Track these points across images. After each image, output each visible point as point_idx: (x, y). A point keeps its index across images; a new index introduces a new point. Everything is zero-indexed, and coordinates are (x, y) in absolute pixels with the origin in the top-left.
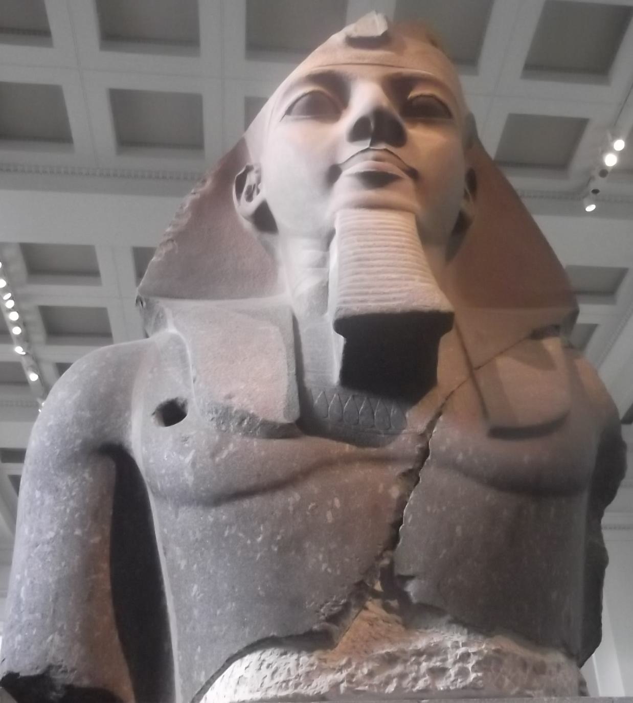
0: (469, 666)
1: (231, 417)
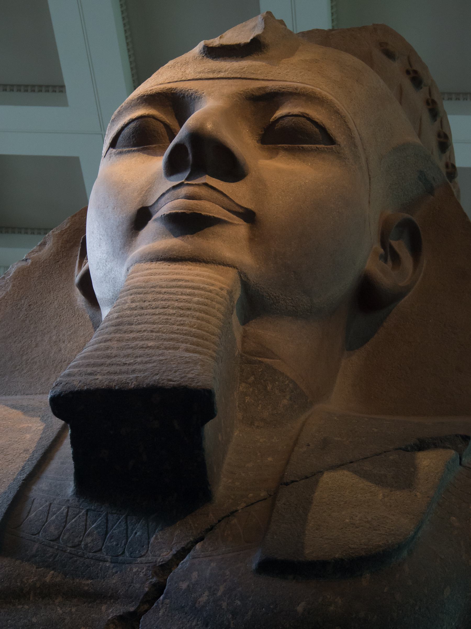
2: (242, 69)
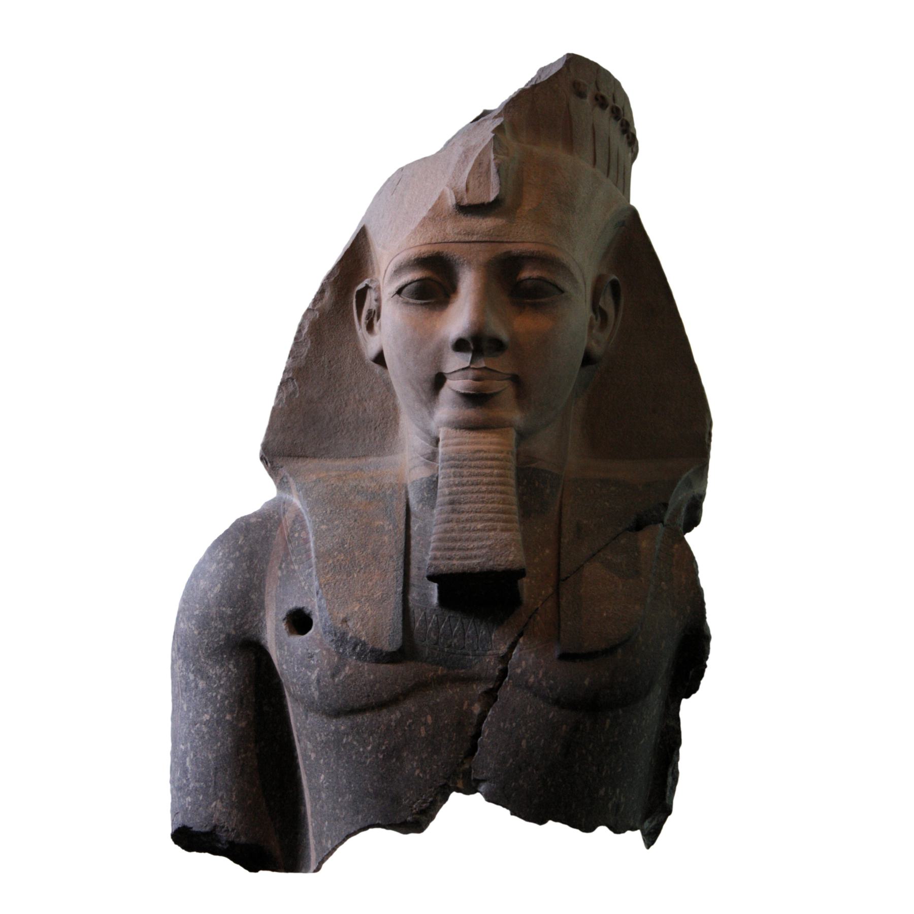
1: (347, 642)
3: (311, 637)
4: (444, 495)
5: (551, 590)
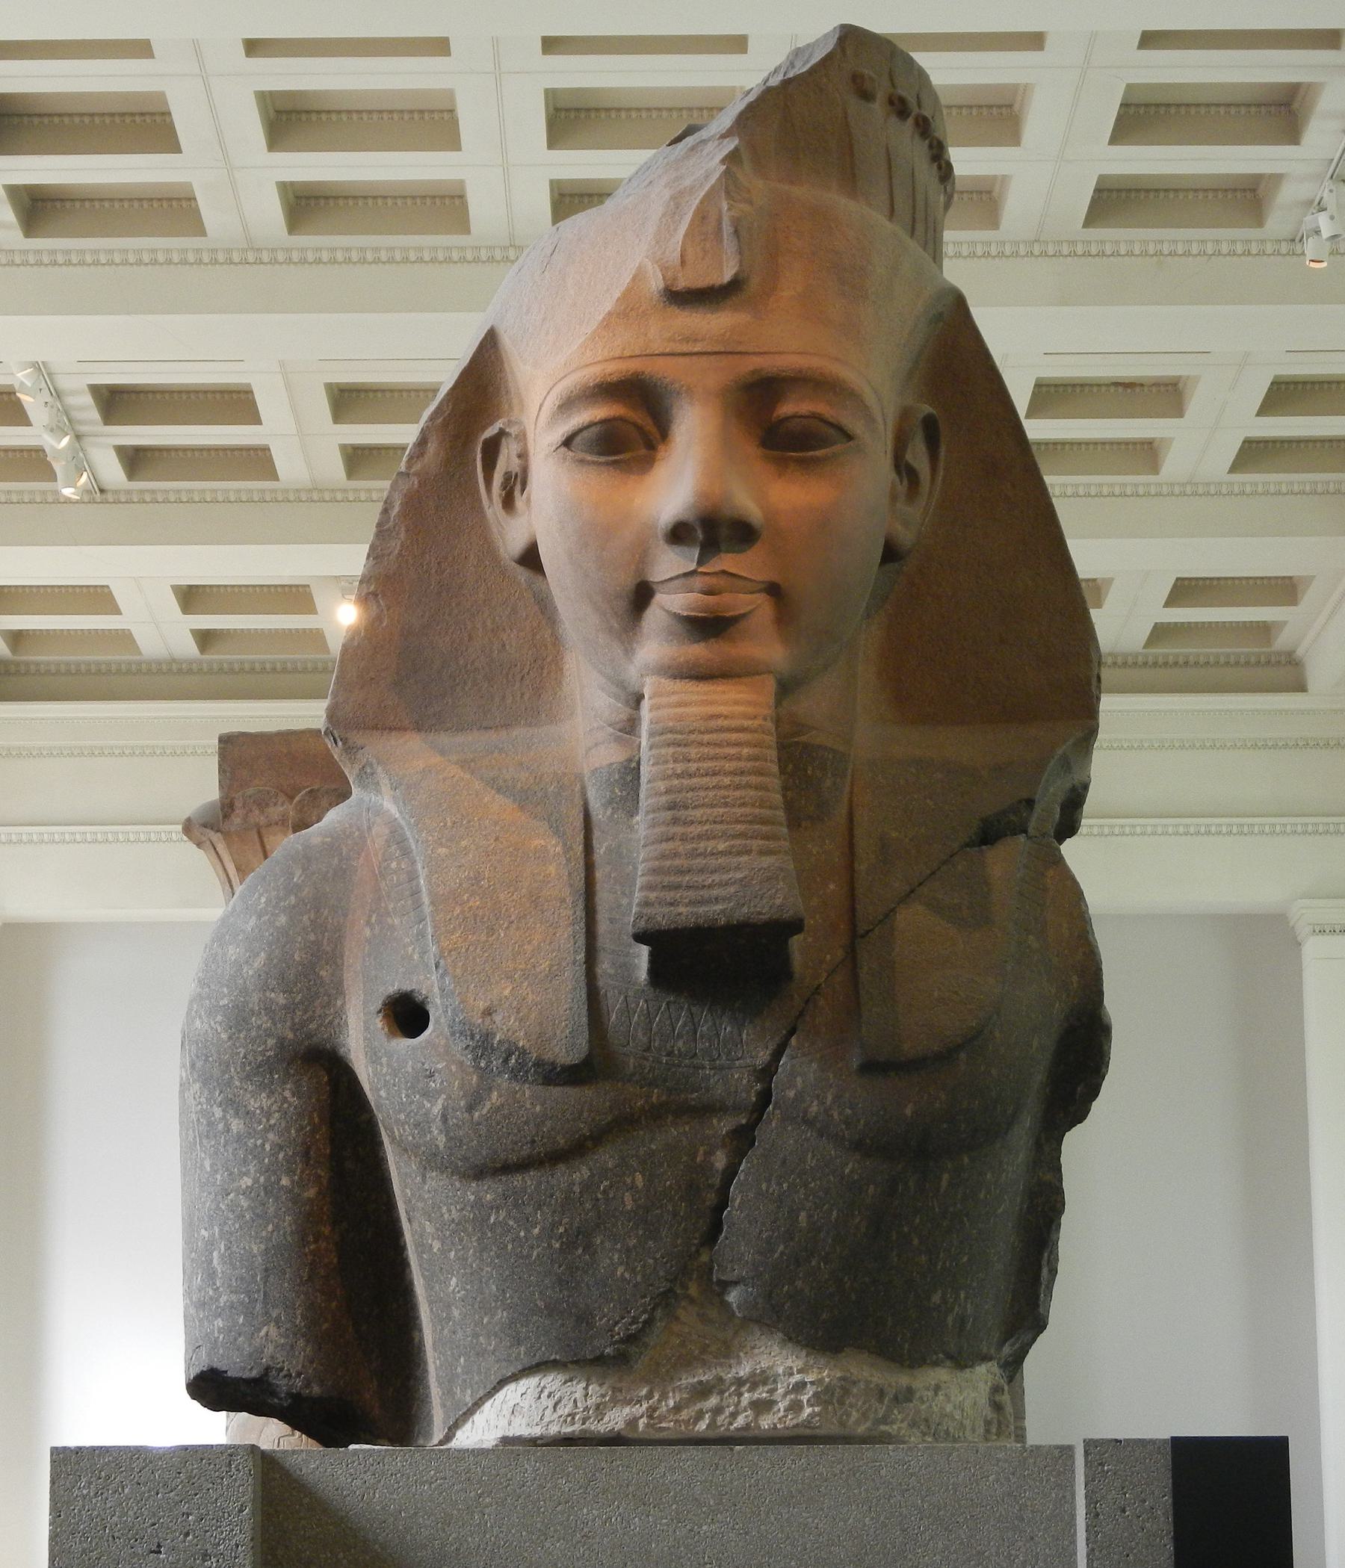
0: (805, 1398)
2: (724, 335)
3: (428, 1042)
4: (658, 794)
5: (840, 954)
